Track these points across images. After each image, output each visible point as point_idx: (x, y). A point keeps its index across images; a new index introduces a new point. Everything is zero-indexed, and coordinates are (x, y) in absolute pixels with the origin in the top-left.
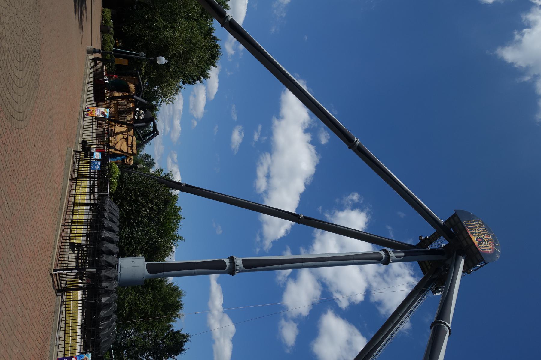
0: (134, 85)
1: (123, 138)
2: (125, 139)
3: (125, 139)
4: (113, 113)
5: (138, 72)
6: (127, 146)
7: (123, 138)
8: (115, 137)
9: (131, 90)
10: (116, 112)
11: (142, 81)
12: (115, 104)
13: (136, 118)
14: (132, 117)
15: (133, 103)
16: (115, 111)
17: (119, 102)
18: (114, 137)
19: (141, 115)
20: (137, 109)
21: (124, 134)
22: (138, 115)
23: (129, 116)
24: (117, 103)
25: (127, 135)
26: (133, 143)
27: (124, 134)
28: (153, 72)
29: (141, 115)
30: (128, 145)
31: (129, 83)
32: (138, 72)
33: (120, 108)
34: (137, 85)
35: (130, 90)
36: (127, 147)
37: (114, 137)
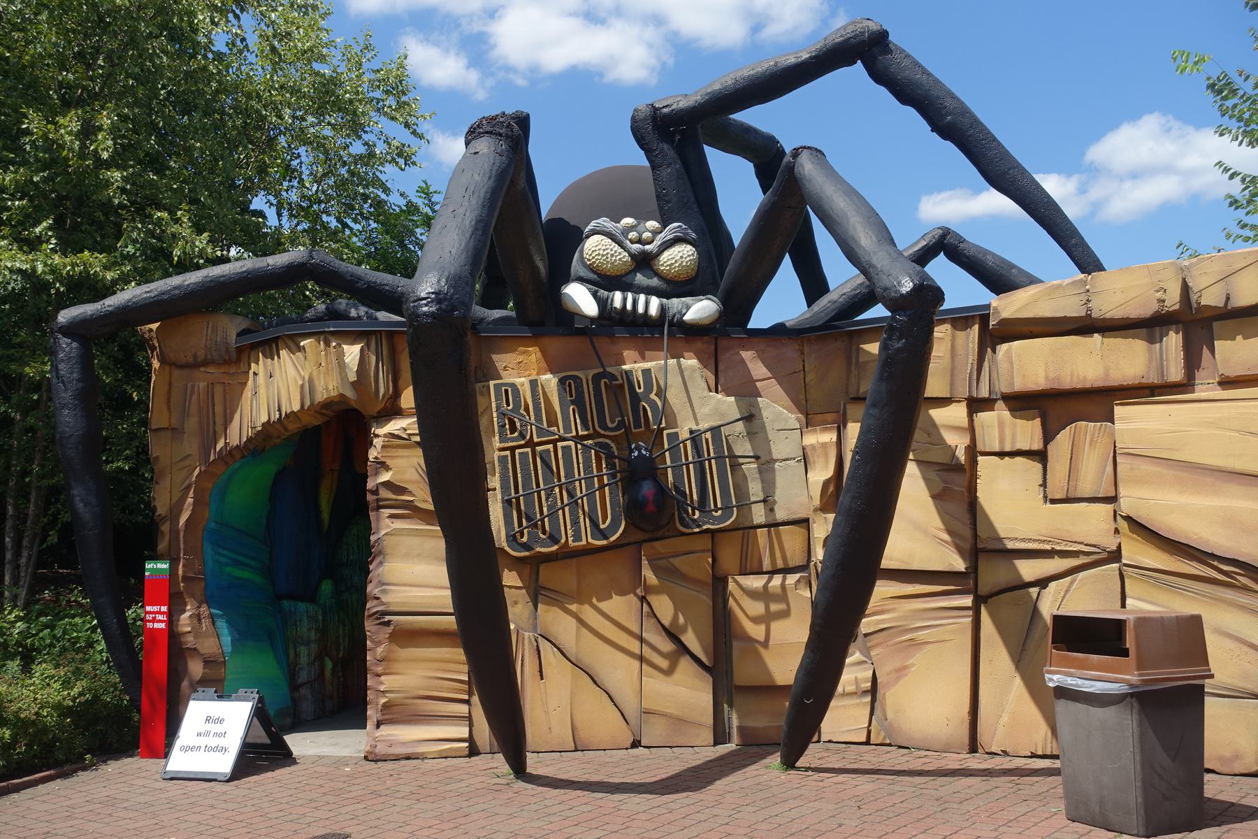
0: (260, 367)
1: (1040, 456)
2: (1048, 436)
3: (1048, 436)
4: (664, 607)
5: (64, 316)
6: (1185, 386)
7: (1040, 456)
8: (1029, 570)
9: (328, 387)
10: (649, 575)
11: (185, 266)
12: (537, 593)
13: (700, 309)
14: (690, 362)
15: (501, 360)
16: (634, 584)
17: (512, 538)
18: (1043, 583)
19: (644, 262)
20: (581, 298)
21: (973, 451)
22: (649, 291)
23: (675, 397)
24: (531, 566)
25: (976, 405)
26: (1143, 308)
27: (973, 451)
28: (53, 146)
29: (644, 262)
30: (1176, 373)
31: (237, 433)
32: (64, 316)
33: (584, 523)
34: (242, 323)
35: (328, 404)
36: (1205, 388)
37: (1043, 583)
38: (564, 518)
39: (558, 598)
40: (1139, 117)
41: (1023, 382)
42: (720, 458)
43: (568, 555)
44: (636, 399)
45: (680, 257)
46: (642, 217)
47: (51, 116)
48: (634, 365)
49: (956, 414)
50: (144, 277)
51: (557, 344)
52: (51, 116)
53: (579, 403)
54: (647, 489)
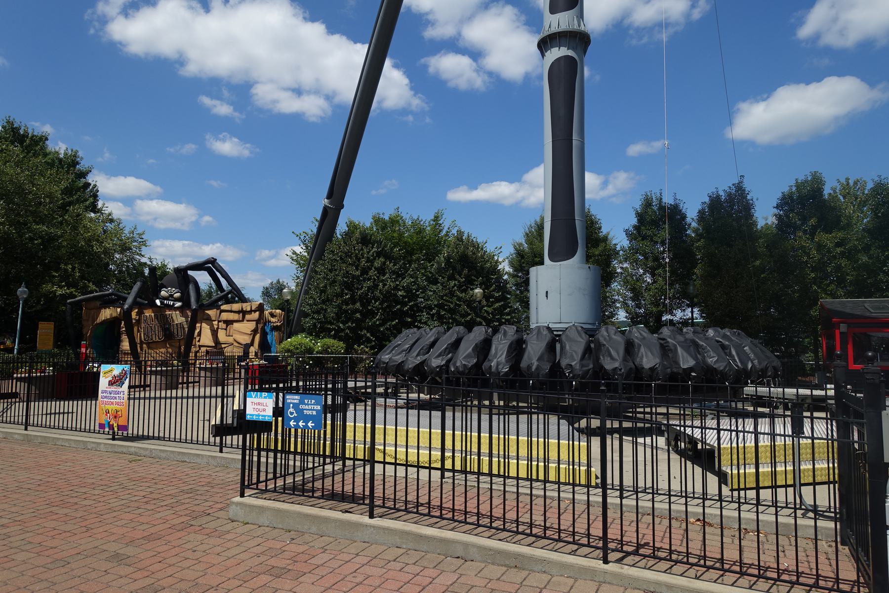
0: (103, 310)
1: (226, 329)
2: (227, 327)
3: (227, 327)
4: (170, 350)
5: (68, 301)
6: (243, 320)
7: (226, 329)
8: (223, 346)
9: (114, 315)
10: (168, 346)
11: (91, 292)
12: (149, 348)
13: (178, 304)
14: (178, 312)
15: (145, 311)
16: (165, 347)
17: (144, 339)
18: (225, 348)
19: (171, 296)
20: (158, 302)
21: (218, 328)
22: (172, 300)
23: (174, 318)
24: (148, 344)
25: (219, 321)
26: (237, 310)
27: (218, 328)
28: (66, 270)
29: (171, 296)
30: (241, 319)
31: (99, 320)
32: (68, 301)
33: (157, 337)
34: (100, 303)
35: (115, 317)
36: (245, 322)
37: (225, 348)
38: (154, 336)
39: (152, 349)
40: (459, 187)
41: (225, 319)
42: (181, 328)
43: (154, 342)
44: (167, 318)
45: (177, 295)
46: (172, 287)
47: (66, 264)
48: (168, 313)
49: (216, 323)
50: (83, 295)
51: (154, 309)
52: (66, 264)
53: (157, 319)
54: (168, 332)
